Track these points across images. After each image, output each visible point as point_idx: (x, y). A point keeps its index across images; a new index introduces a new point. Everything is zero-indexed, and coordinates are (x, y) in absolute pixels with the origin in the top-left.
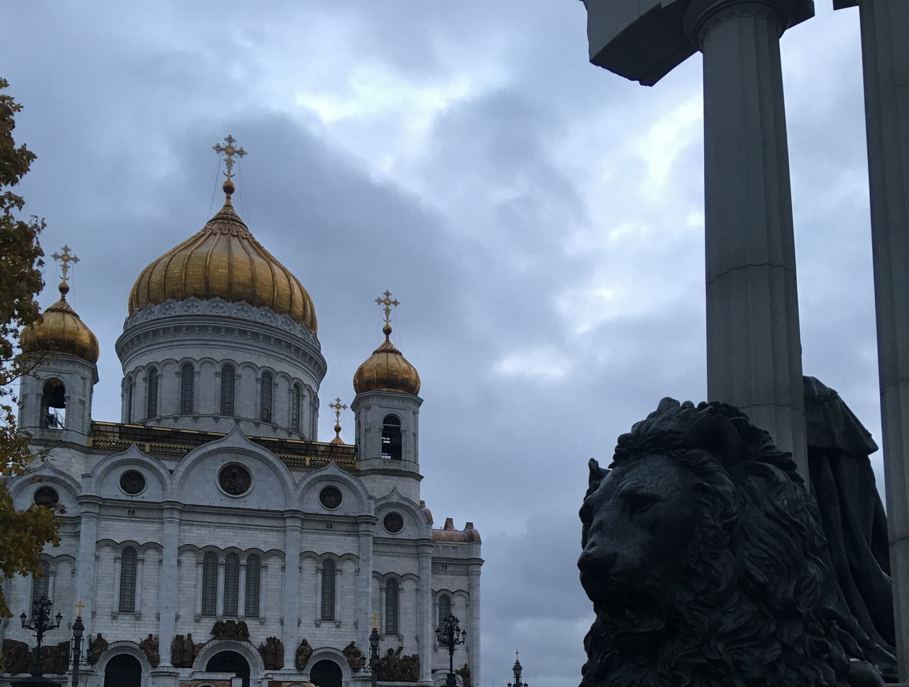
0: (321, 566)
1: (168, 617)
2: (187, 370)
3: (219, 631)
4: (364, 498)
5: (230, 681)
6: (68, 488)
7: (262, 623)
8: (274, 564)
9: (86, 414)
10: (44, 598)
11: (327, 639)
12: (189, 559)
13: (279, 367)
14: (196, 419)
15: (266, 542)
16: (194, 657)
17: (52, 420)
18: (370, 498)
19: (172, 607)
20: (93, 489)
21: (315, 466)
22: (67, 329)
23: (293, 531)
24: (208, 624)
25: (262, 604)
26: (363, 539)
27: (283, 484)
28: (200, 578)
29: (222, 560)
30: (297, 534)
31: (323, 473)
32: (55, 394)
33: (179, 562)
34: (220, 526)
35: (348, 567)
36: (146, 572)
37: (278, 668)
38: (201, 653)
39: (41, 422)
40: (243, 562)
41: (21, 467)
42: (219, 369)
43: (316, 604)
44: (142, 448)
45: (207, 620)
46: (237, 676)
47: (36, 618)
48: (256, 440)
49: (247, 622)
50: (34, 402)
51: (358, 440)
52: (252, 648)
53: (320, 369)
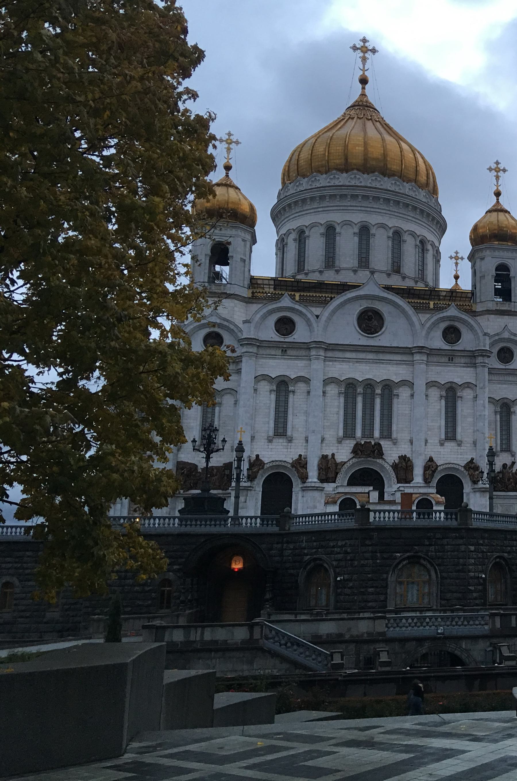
0: (444, 393)
1: (314, 439)
2: (330, 232)
3: (358, 450)
4: (481, 334)
5: (368, 493)
6: (231, 332)
7: (395, 444)
8: (404, 393)
9: (246, 269)
10: (211, 425)
11: (451, 456)
12: (332, 390)
13: (406, 226)
14: (337, 271)
15: (396, 374)
16: (337, 474)
17: (218, 276)
18: (485, 334)
19: (318, 430)
20: (252, 332)
21: (438, 309)
22: (230, 201)
23: (420, 364)
24: (350, 444)
25: (394, 428)
26: (479, 369)
27: (411, 324)
28: (342, 405)
29: (360, 390)
30: (423, 366)
31: (445, 314)
32: (220, 254)
33: (324, 392)
34: (359, 361)
35: (467, 394)
36: (297, 400)
37: (409, 482)
38: (344, 469)
39: (209, 277)
40: (378, 391)
41: (198, 315)
42: (356, 230)
43: (440, 426)
44: (293, 297)
45: (348, 442)
46: (374, 489)
47: (205, 442)
48: (388, 288)
49: (382, 443)
50: (205, 260)
51: (474, 286)
52: (386, 465)
53: (441, 227)
